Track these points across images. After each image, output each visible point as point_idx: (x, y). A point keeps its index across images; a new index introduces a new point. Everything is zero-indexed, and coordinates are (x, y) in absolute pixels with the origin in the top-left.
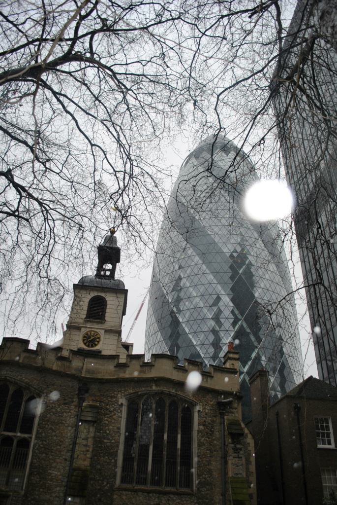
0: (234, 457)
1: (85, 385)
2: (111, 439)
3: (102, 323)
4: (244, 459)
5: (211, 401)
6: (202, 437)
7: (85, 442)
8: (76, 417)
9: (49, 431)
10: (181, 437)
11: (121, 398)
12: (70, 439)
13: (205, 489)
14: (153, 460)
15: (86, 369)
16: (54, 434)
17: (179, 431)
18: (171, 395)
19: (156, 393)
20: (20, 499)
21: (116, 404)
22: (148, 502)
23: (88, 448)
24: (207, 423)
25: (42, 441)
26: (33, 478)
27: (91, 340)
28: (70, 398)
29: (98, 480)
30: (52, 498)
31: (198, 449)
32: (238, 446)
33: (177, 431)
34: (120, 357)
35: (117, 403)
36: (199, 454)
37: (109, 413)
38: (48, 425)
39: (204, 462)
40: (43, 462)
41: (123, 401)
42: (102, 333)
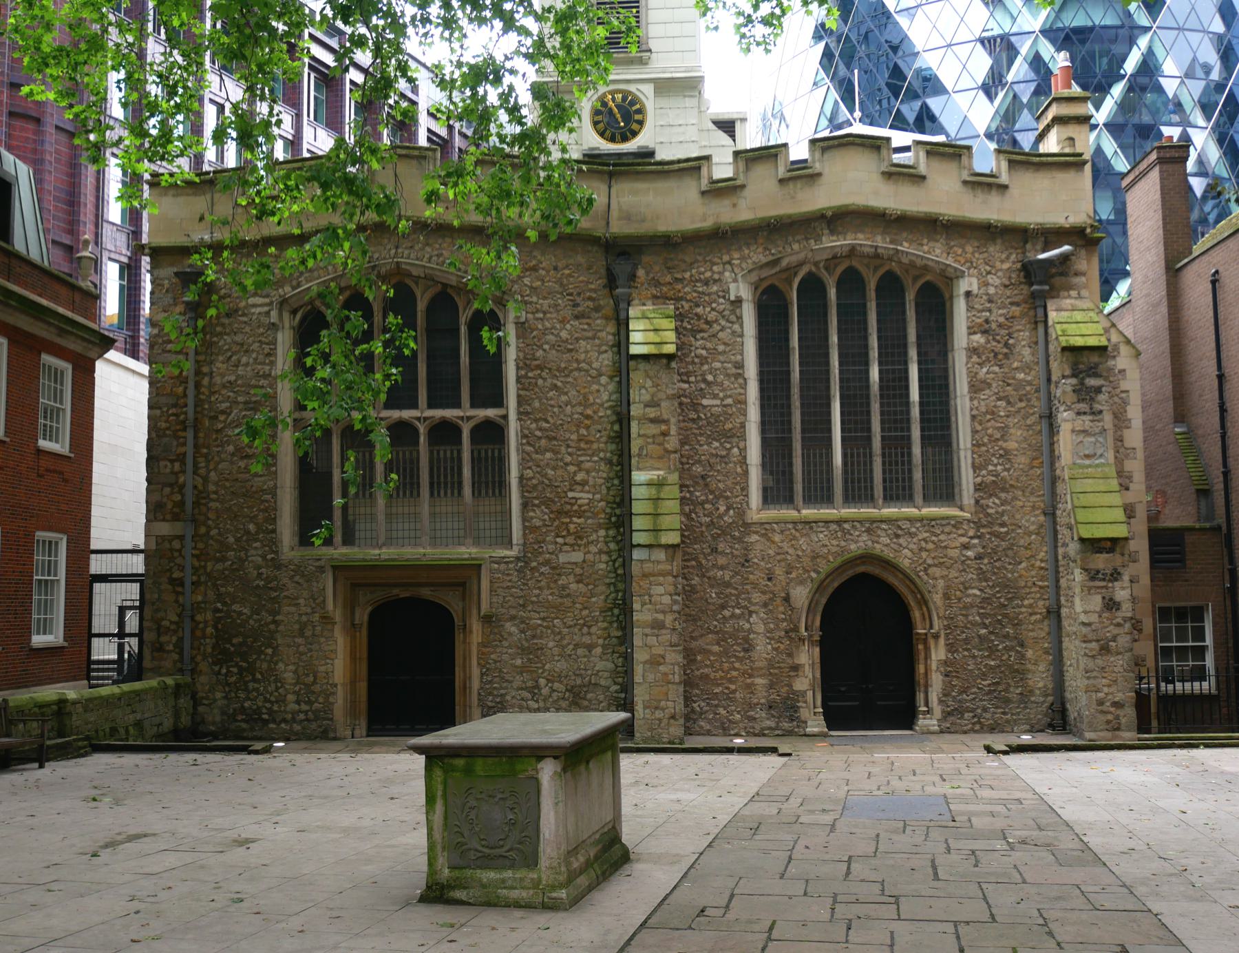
0: (1078, 414)
1: (623, 259)
2: (721, 395)
4: (1108, 418)
5: (1002, 262)
6: (981, 365)
7: (652, 413)
8: (615, 349)
9: (551, 394)
10: (920, 370)
11: (735, 281)
12: (610, 407)
13: (997, 501)
14: (844, 440)
15: (620, 210)
16: (564, 398)
17: (913, 353)
18: (877, 256)
19: (835, 259)
20: (511, 566)
21: (721, 300)
22: (843, 543)
23: (664, 427)
24: (994, 326)
25: (536, 421)
26: (531, 514)
28: (590, 298)
29: (702, 504)
30: (590, 557)
31: (971, 399)
33: (906, 353)
34: (715, 160)
35: (724, 297)
36: (975, 412)
37: (705, 327)
38: (544, 379)
39: (990, 431)
40: (551, 472)
41: (742, 290)
42: (646, 93)
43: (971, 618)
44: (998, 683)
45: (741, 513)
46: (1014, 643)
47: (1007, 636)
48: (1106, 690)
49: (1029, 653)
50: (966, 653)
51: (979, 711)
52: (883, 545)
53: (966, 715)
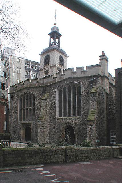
3: (49, 65)
27: (47, 73)
32: (94, 98)
45: (55, 117)
52: (71, 121)
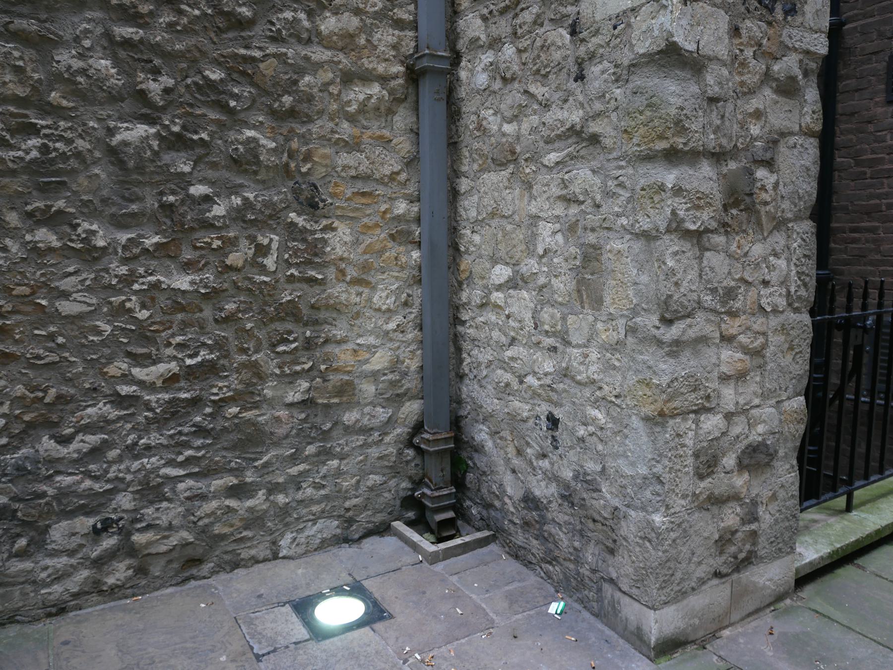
43: (65, 58)
44: (210, 369)
46: (279, 195)
47: (245, 162)
48: (729, 396)
49: (340, 240)
50: (45, 236)
51: (125, 501)
53: (58, 532)
